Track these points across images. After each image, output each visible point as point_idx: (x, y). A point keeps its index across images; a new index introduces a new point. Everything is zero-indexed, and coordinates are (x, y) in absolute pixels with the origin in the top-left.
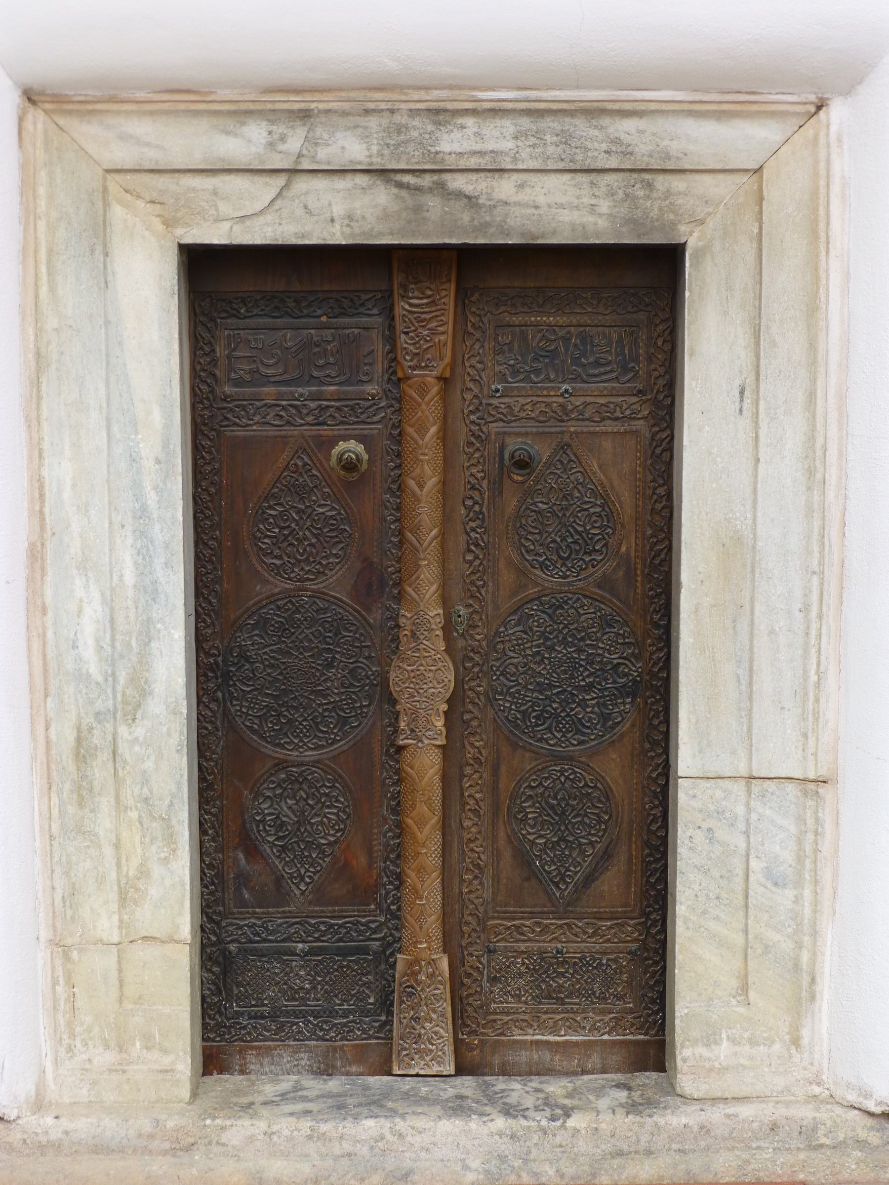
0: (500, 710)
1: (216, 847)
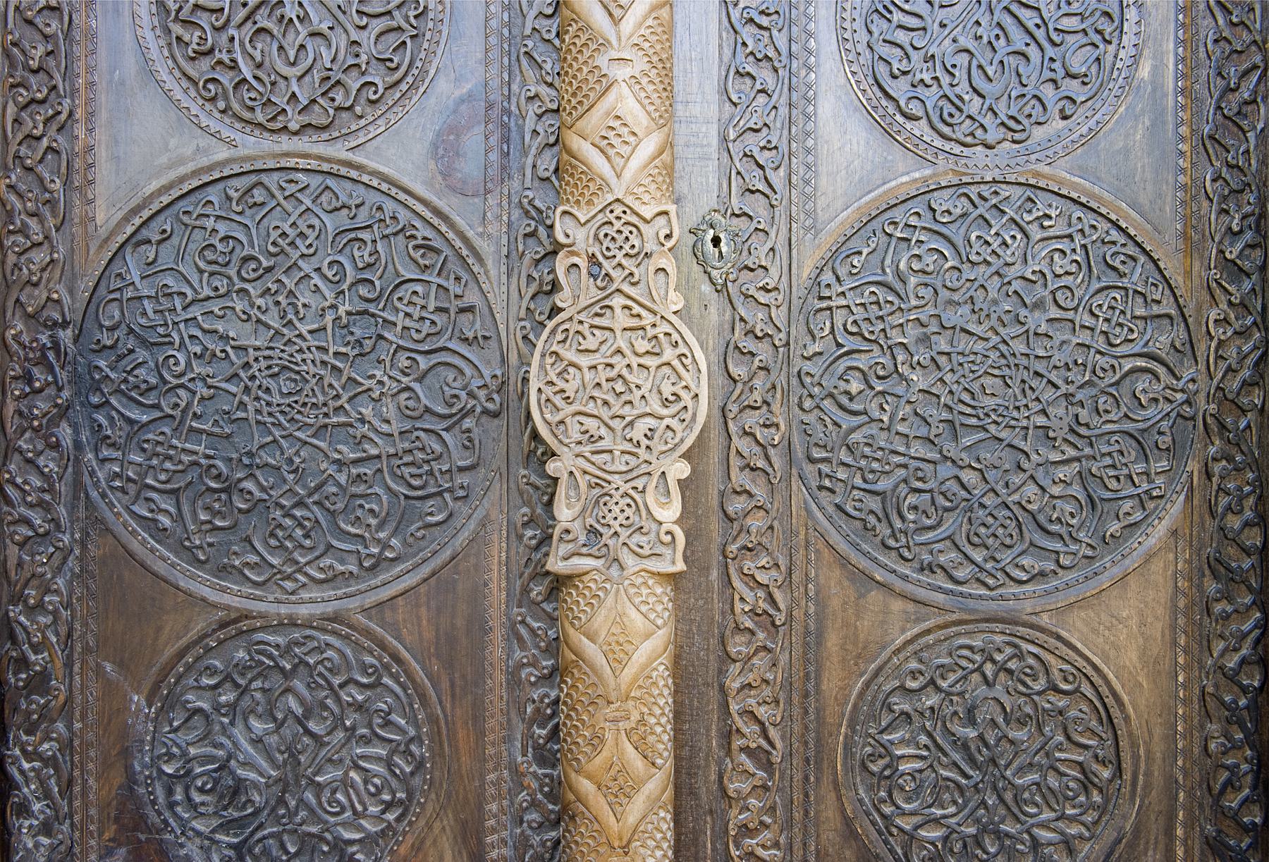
0: (821, 488)
1: (53, 848)
